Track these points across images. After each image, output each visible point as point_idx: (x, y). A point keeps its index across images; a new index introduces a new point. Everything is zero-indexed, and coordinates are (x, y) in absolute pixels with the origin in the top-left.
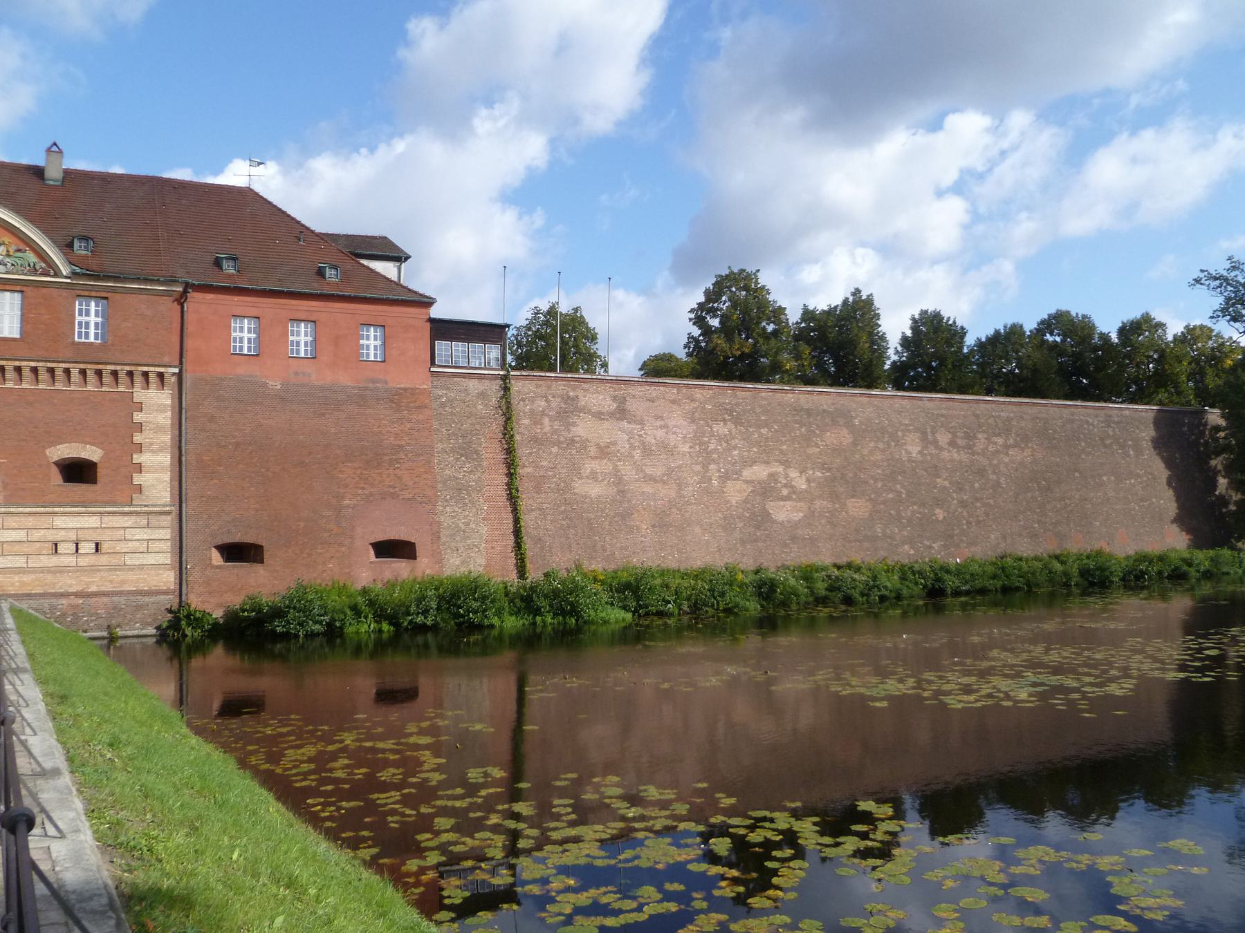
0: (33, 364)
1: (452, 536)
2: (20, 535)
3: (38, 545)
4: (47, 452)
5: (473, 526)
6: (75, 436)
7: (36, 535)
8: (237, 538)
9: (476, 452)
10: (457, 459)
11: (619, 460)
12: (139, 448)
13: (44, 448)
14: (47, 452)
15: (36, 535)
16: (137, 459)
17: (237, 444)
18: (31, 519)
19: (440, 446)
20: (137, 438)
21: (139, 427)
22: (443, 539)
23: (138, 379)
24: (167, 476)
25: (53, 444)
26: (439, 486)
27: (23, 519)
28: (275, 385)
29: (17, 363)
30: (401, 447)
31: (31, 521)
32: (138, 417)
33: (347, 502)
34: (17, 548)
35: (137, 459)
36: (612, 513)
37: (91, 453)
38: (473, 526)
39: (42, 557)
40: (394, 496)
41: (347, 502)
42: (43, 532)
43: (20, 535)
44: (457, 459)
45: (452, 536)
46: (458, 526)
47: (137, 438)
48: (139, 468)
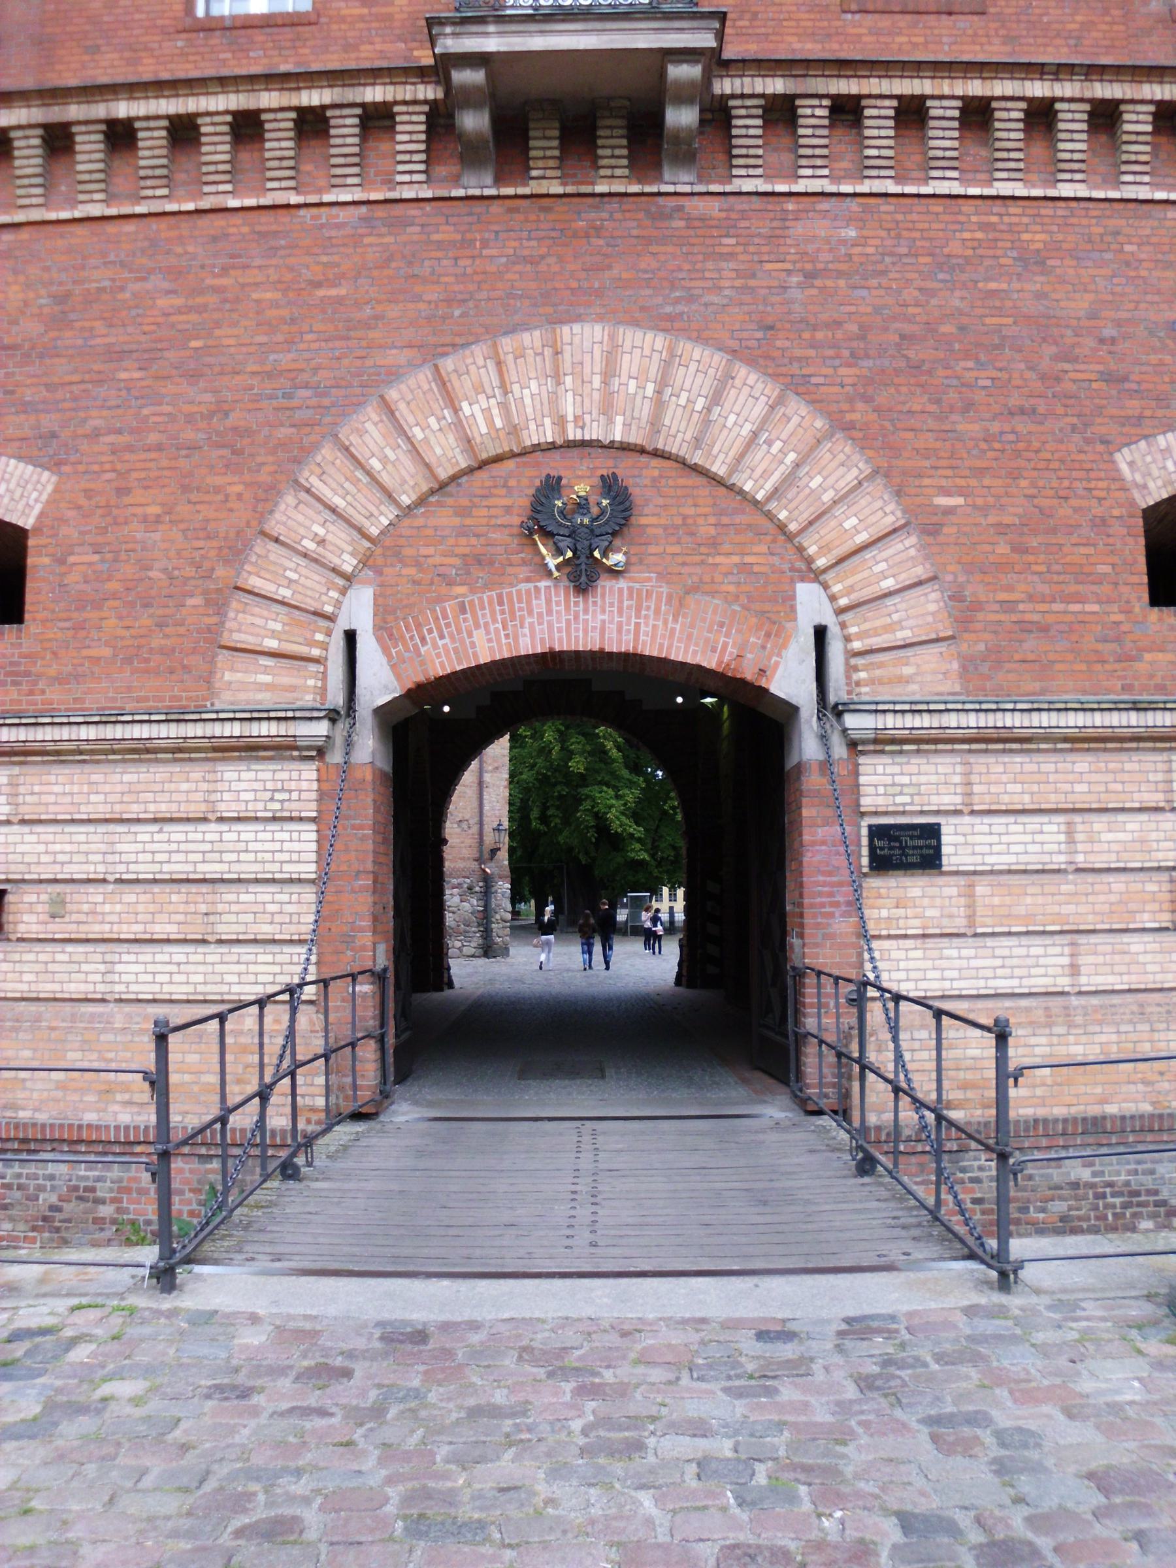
0: (1038, 89)
2: (1042, 841)
3: (1118, 883)
4: (1122, 459)
7: (1110, 839)
13: (1110, 445)
14: (1122, 459)
15: (1110, 839)
18: (1082, 763)
25: (1139, 428)
27: (1048, 764)
29: (975, 88)
31: (1081, 777)
34: (1034, 902)
39: (1135, 943)
42: (1133, 824)
43: (1042, 841)
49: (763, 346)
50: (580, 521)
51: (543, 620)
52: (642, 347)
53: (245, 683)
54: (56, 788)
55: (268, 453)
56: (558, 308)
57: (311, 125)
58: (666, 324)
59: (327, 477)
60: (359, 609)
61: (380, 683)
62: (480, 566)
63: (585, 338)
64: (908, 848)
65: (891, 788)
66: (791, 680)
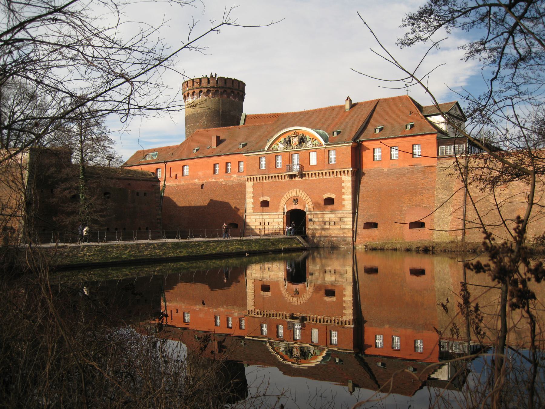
1: (438, 220)
5: (446, 216)
6: (329, 191)
8: (371, 221)
9: (451, 188)
10: (443, 191)
11: (513, 188)
12: (343, 194)
16: (343, 197)
17: (373, 190)
19: (437, 187)
20: (343, 191)
21: (343, 188)
22: (435, 221)
23: (342, 173)
24: (351, 202)
25: (324, 194)
26: (436, 202)
28: (386, 169)
30: (424, 188)
32: (343, 184)
33: (404, 208)
35: (343, 197)
36: (506, 211)
37: (333, 196)
38: (446, 216)
40: (420, 206)
41: (404, 208)
44: (443, 191)
45: (438, 220)
46: (440, 216)
47: (343, 191)
48: (344, 200)
49: (305, 190)
50: (296, 201)
51: (293, 207)
52: (298, 190)
53: (280, 210)
54: (271, 217)
55: (281, 197)
56: (294, 188)
57: (281, 176)
58: (299, 188)
59: (283, 199)
60: (285, 206)
61: (286, 211)
62: (291, 204)
63: (295, 190)
64: (311, 220)
65: (310, 217)
66: (305, 210)
